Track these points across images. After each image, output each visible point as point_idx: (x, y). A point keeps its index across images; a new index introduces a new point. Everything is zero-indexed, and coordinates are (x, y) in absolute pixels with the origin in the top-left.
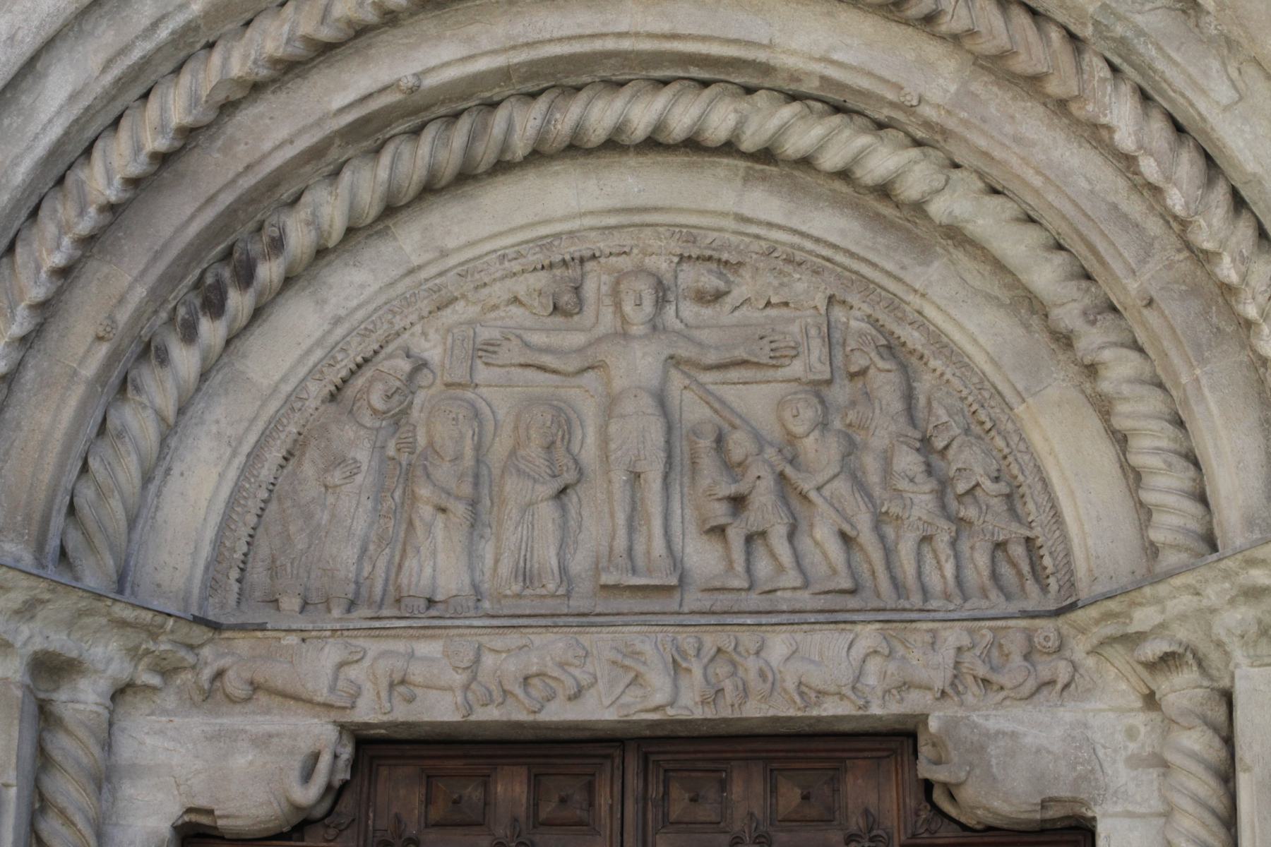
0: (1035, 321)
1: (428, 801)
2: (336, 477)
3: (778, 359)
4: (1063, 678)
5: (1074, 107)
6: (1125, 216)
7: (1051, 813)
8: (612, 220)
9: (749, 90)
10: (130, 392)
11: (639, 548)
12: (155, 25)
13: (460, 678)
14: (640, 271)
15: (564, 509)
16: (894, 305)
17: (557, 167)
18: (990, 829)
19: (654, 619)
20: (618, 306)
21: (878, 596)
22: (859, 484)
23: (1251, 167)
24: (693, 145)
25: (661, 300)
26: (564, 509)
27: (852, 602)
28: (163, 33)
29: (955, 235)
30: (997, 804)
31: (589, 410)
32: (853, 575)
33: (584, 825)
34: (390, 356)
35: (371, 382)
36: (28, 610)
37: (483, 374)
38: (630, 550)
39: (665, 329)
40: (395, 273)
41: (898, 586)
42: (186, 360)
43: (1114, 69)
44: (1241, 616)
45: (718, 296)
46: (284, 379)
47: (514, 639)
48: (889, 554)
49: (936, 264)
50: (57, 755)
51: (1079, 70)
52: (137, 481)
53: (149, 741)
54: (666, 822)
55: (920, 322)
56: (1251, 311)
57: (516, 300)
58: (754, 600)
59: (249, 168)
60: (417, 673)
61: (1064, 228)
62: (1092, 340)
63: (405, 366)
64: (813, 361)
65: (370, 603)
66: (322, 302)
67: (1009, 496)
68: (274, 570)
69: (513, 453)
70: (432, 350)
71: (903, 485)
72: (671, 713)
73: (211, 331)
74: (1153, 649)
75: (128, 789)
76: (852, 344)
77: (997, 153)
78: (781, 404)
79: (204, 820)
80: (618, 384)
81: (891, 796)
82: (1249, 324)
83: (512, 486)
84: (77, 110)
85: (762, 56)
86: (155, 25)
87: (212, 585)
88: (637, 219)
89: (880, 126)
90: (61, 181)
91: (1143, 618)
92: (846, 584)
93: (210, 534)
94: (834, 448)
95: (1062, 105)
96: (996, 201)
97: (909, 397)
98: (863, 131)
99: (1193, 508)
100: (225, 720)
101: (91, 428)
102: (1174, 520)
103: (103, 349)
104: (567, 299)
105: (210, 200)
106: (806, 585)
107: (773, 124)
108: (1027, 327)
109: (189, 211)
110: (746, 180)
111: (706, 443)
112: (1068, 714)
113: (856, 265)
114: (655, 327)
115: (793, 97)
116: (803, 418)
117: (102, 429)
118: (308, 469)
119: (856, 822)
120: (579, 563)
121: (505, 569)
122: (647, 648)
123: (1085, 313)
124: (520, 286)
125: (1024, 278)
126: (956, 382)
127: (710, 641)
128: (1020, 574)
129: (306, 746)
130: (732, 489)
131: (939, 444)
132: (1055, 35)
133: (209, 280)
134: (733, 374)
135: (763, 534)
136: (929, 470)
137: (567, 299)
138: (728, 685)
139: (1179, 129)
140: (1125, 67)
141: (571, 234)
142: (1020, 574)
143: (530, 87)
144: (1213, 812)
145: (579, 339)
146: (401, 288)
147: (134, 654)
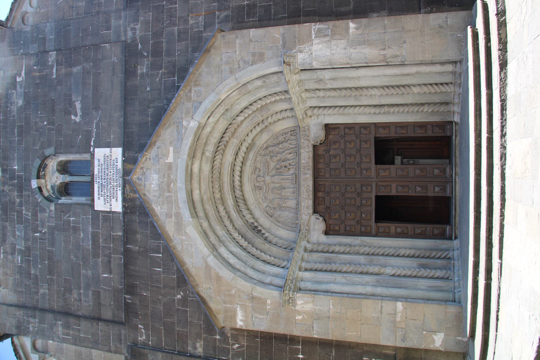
0: (264, 130)
1: (322, 205)
2: (281, 216)
3: (267, 162)
4: (308, 127)
5: (238, 125)
6: (252, 119)
7: (324, 129)
8: (250, 182)
9: (234, 165)
10: (271, 241)
11: (291, 179)
12: (226, 237)
13: (307, 200)
14: (256, 179)
15: (286, 188)
16: (261, 148)
17: (243, 189)
18: (325, 136)
19: (300, 176)
20: (261, 181)
21: (297, 150)
22: (283, 152)
23: (247, 103)
24: (241, 172)
25: (260, 176)
26: (286, 188)
27: (298, 153)
28: (227, 236)
29: (253, 140)
30: (323, 135)
31: (274, 185)
32: (294, 153)
33: (324, 185)
34: (266, 210)
35: (269, 212)
36: (298, 252)
37: (269, 198)
38: (291, 180)
39: (264, 176)
40: (256, 209)
41: (296, 147)
42: (267, 234)
43: (234, 120)
44: (301, 105)
45: (259, 169)
46: (269, 223)
47: (302, 194)
48: (292, 148)
49: (256, 142)
50: (316, 249)
51: (234, 124)
52: (281, 240)
53: (314, 239)
54: (324, 175)
55: (263, 144)
56: (264, 103)
57: (260, 194)
58: (297, 165)
59: (243, 226)
60: (306, 205)
61: (253, 126)
62: (266, 123)
63: (268, 208)
64: (268, 158)
65: (297, 212)
66: (260, 218)
67: (285, 134)
68: (293, 224)
69: (278, 194)
70: (266, 204)
71: (283, 146)
72: (311, 174)
73: (263, 231)
74: (305, 116)
75: (320, 241)
76: (266, 153)
77: (243, 134)
78: (273, 162)
79: (324, 232)
80: (270, 182)
81: (322, 148)
82: (266, 104)
83: (283, 194)
84: (237, 247)
85: (231, 163)
86: (226, 237)
87: (294, 231)
88: (250, 179)
89: (239, 149)
90: (245, 249)
91: (301, 117)
92: (295, 153)
93: (288, 232)
94: (279, 155)
95: (238, 126)
96: (249, 135)
97: (272, 146)
98: (240, 151)
99: (287, 111)
100: (312, 229)
101: (276, 246)
102: (289, 113)
103: (266, 244)
104: (259, 188)
106: (295, 158)
107: (239, 162)
108: (264, 131)
109: (248, 234)
110: (245, 166)
111: (278, 171)
112: (312, 127)
113: (257, 151)
114: (263, 177)
115: (235, 159)
116: (275, 159)
117: (275, 245)
118: (280, 220)
119: (324, 152)
120: (292, 186)
121: (293, 195)
122: (303, 177)
123: (263, 124)
125: (258, 131)
126: (271, 140)
127: (302, 170)
128: (294, 133)
129: (315, 219)
130: (284, 167)
131: (278, 142)
132: (229, 127)
133: (257, 232)
134: (269, 167)
135: (289, 164)
136: (282, 143)
137: (259, 188)
138: (308, 168)
139: (241, 112)
140: (234, 118)
141: (252, 187)
142: (294, 133)
143: (233, 192)
144: (324, 109)
145: (264, 187)
146: (258, 209)
147: (304, 240)
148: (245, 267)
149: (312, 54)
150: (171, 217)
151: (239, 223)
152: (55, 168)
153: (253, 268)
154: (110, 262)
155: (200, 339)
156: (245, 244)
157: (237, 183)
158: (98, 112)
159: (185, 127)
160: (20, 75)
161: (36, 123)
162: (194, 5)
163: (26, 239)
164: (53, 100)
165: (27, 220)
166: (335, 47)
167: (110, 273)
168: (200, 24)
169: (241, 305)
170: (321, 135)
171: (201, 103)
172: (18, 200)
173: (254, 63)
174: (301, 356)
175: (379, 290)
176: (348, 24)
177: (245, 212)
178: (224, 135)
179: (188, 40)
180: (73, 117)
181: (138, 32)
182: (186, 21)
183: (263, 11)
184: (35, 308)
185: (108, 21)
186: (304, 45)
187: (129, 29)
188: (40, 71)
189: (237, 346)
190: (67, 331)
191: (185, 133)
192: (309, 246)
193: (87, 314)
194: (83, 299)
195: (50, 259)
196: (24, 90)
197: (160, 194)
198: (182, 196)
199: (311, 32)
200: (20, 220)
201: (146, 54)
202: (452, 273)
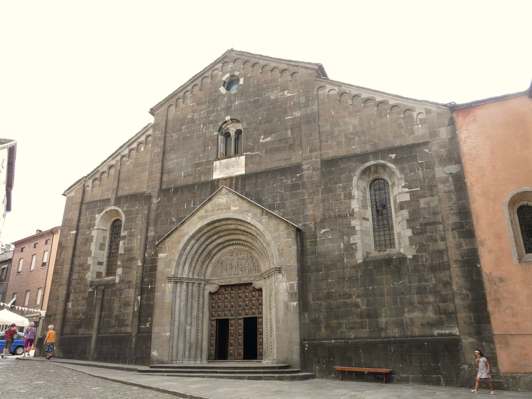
37: (227, 260)
42: (207, 262)
45: (241, 254)
148: (186, 255)
149: (281, 282)
150: (206, 213)
151: (211, 247)
153: (186, 259)
154: (189, 176)
155: (155, 233)
156: (199, 252)
157: (232, 243)
158: (264, 154)
159: (248, 215)
160: (288, 93)
161: (260, 112)
164: (272, 121)
165: (209, 117)
166: (284, 295)
167: (184, 177)
168: (308, 212)
170: (257, 287)
172: (219, 109)
173: (278, 250)
174: (150, 286)
175: (176, 323)
176: (296, 301)
177: (217, 249)
178: (251, 234)
180: (262, 137)
181: (307, 172)
182: (311, 203)
184: (166, 132)
185: (315, 150)
188: (290, 107)
189: (153, 253)
191: (245, 215)
193: (165, 165)
194: (171, 162)
195: (190, 137)
196: (280, 98)
198: (215, 218)
200: (209, 113)
201: (293, 180)
202: (186, 360)
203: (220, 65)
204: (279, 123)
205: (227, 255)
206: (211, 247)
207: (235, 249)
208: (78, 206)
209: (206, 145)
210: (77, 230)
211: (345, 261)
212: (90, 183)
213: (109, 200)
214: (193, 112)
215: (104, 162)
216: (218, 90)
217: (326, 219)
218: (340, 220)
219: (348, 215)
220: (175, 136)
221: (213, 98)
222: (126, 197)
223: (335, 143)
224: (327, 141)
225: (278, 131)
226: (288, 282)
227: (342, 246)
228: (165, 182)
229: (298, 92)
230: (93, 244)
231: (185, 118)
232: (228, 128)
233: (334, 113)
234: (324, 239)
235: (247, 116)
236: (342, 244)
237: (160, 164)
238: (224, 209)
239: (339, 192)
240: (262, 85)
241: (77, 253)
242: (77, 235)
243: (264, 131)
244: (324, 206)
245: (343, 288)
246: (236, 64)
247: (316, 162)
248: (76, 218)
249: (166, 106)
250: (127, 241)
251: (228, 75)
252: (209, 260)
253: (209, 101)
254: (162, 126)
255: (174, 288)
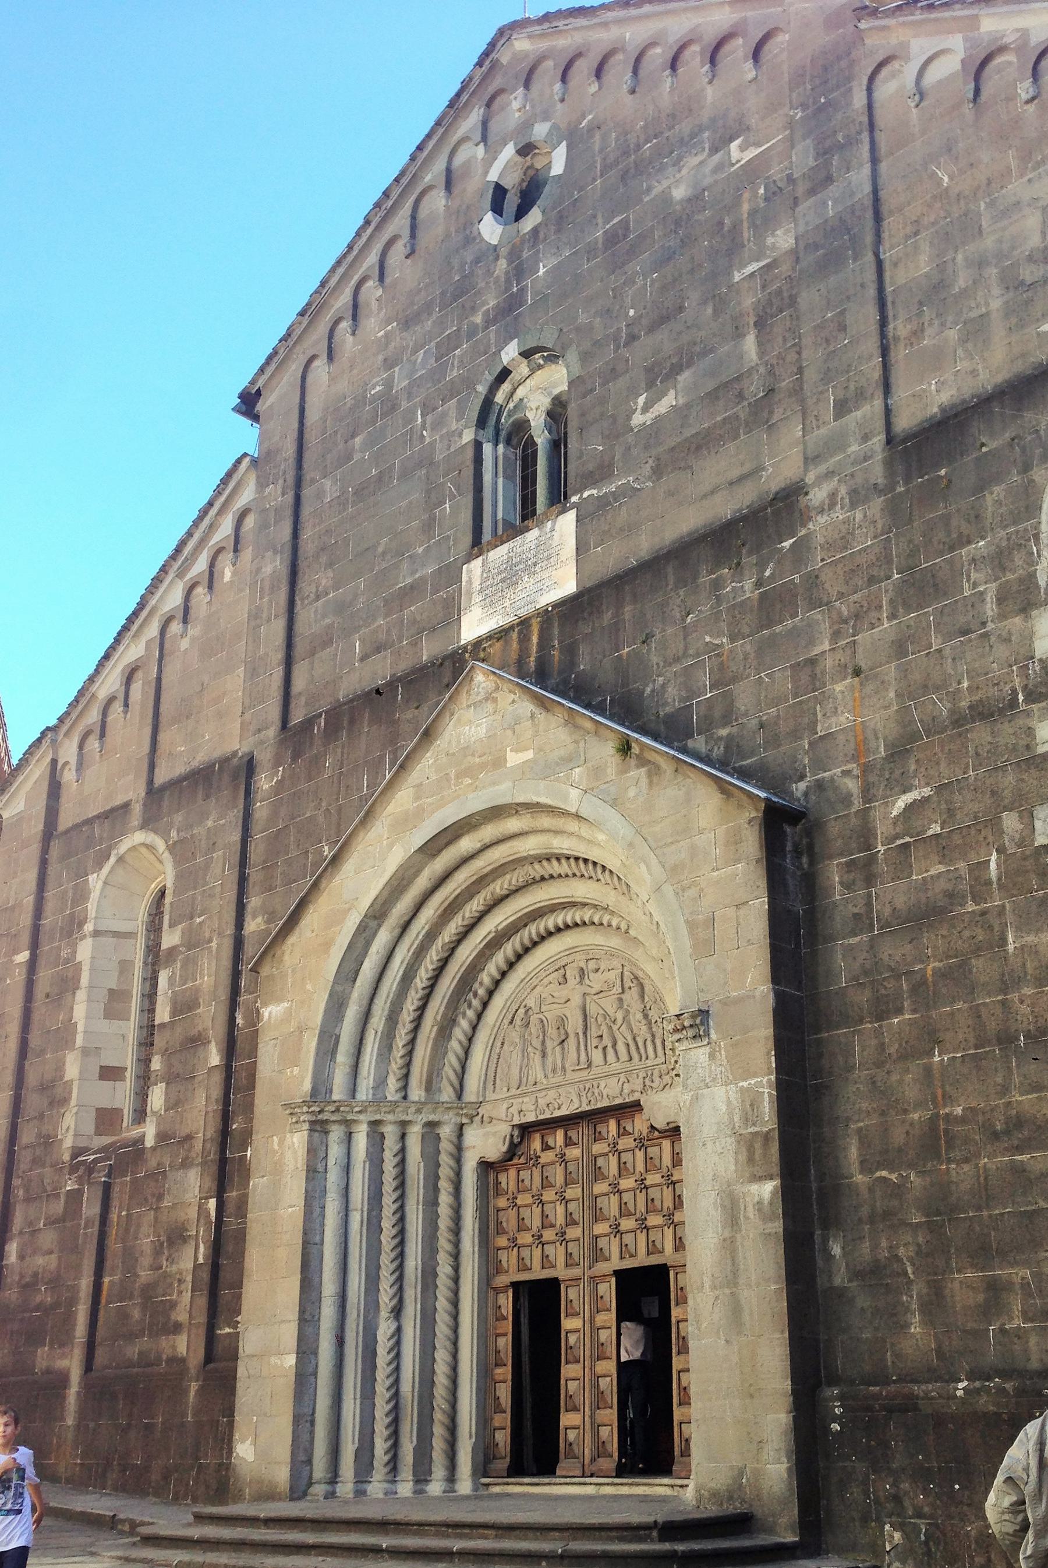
13: (533, 1107)
26: (563, 1049)
28: (420, 937)
40: (518, 981)
42: (464, 1024)
105: (454, 977)
118: (505, 1046)
124: (550, 978)
151: (466, 953)
152: (556, 391)
155: (268, 922)
158: (649, 478)
160: (742, 149)
162: (883, 682)
163: (409, 392)
168: (834, 719)
169: (291, 1008)
171: (614, 803)
172: (478, 319)
173: (691, 925)
179: (796, 695)
180: (641, 400)
181: (822, 519)
183: (856, 910)
186: (725, 1062)
187: (834, 482)
190: (267, 589)
191: (558, 780)
192: (446, 1132)
195: (380, 478)
197: (454, 754)
199: (755, 1075)
201: (767, 573)
203: (475, 115)
204: (710, 311)
205: (546, 981)
206: (466, 953)
207: (572, 950)
208: (35, 849)
209: (433, 498)
210: (34, 946)
211: (1011, 948)
212: (69, 752)
213: (126, 806)
214: (389, 364)
215: (107, 657)
216: (475, 233)
217: (915, 737)
218: (980, 735)
219: (1021, 698)
220: (330, 488)
221: (457, 278)
222: (175, 784)
223: (952, 335)
224: (918, 333)
225: (705, 353)
226: (736, 1080)
227: (993, 865)
228: (300, 694)
229: (785, 128)
230: (81, 995)
231: (361, 400)
232: (521, 400)
233: (951, 178)
234: (906, 845)
235: (583, 318)
236: (994, 857)
237: (279, 626)
238: (482, 767)
239: (975, 585)
240: (638, 147)
241: (35, 1040)
242: (32, 965)
243: (648, 370)
244: (904, 672)
245: (1005, 1090)
246: (536, 86)
247: (866, 459)
248: (29, 901)
249: (294, 369)
250: (179, 965)
251: (509, 152)
252: (471, 1014)
253: (443, 293)
254: (286, 460)
255: (311, 1151)
